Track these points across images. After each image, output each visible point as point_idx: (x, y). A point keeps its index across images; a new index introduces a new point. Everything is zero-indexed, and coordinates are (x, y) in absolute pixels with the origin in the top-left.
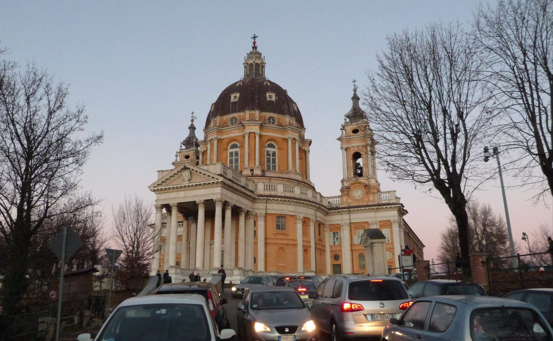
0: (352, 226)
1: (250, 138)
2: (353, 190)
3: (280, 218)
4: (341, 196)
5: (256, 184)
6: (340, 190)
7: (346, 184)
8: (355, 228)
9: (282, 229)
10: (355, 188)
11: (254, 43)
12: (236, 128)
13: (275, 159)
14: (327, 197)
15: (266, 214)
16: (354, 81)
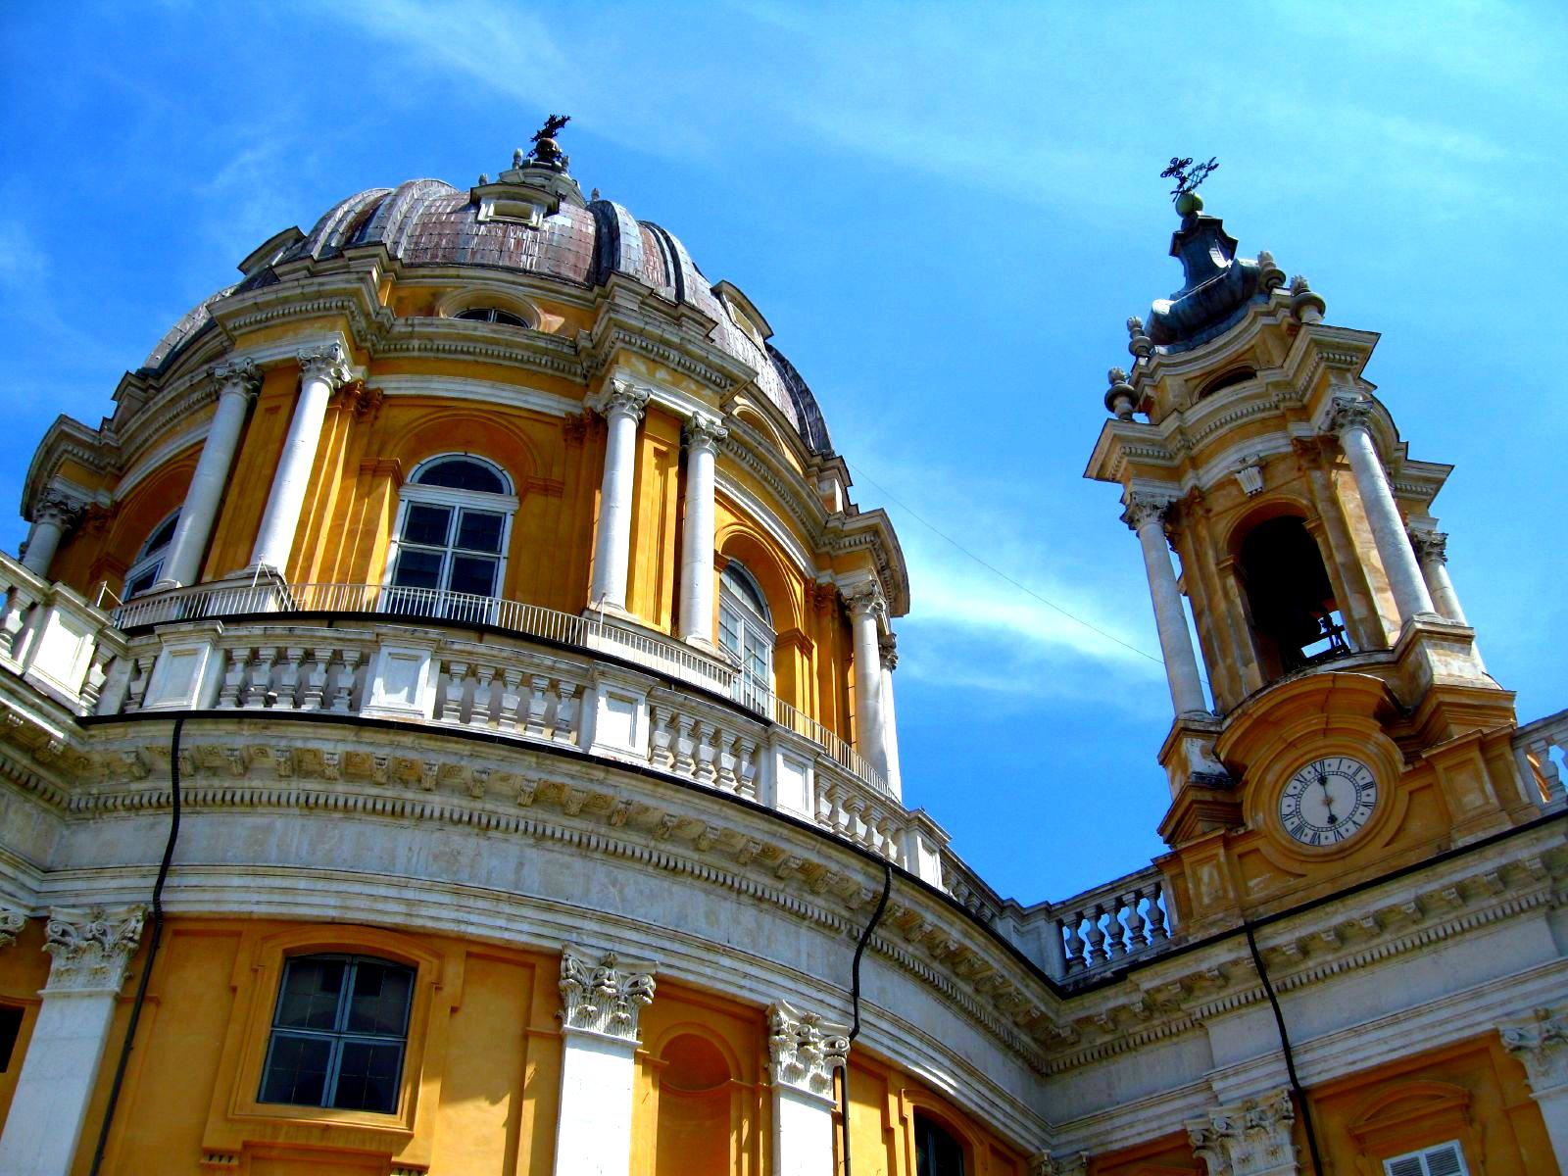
0: (1332, 1123)
1: (261, 406)
2: (1270, 777)
3: (349, 981)
4: (1174, 858)
5: (144, 663)
6: (1161, 831)
7: (1197, 757)
8: (1359, 1140)
9: (348, 1101)
10: (1294, 754)
11: (545, 152)
12: (196, 396)
13: (490, 567)
14: (1048, 910)
15: (157, 922)
16: (1176, 168)
